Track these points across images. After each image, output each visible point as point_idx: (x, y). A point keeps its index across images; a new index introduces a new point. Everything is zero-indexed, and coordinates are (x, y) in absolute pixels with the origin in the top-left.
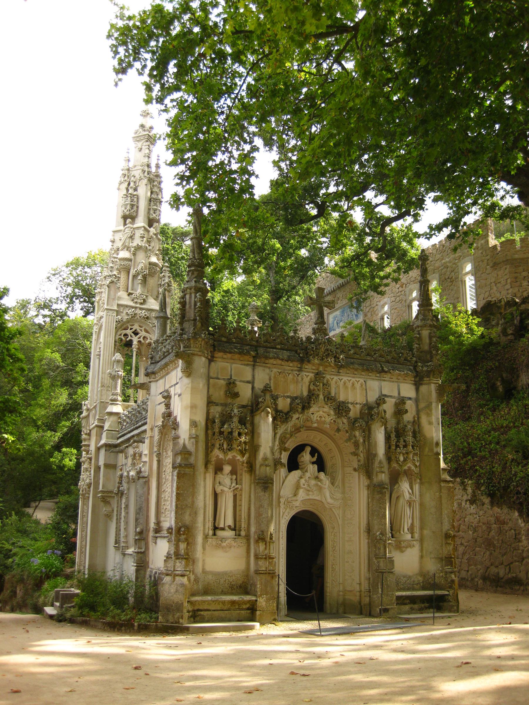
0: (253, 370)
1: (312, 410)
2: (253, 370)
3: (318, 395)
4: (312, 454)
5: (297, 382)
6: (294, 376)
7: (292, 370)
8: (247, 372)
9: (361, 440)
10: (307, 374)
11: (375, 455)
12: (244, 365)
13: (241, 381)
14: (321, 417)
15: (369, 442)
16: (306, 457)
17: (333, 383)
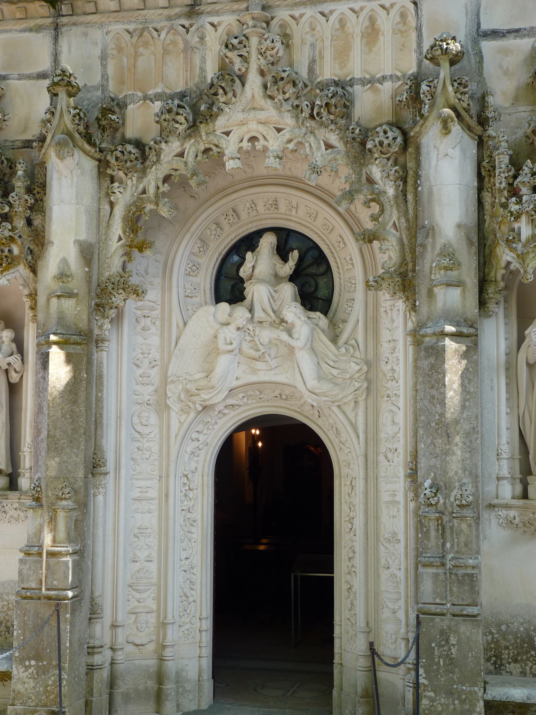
0: (56, 39)
1: (221, 123)
2: (56, 39)
3: (242, 79)
4: (282, 253)
5: (188, 49)
6: (177, 33)
7: (169, 18)
8: (38, 50)
9: (391, 192)
10: (215, 20)
11: (431, 231)
12: (31, 30)
13: (21, 77)
14: (253, 139)
15: (416, 194)
16: (262, 262)
17: (298, 32)
